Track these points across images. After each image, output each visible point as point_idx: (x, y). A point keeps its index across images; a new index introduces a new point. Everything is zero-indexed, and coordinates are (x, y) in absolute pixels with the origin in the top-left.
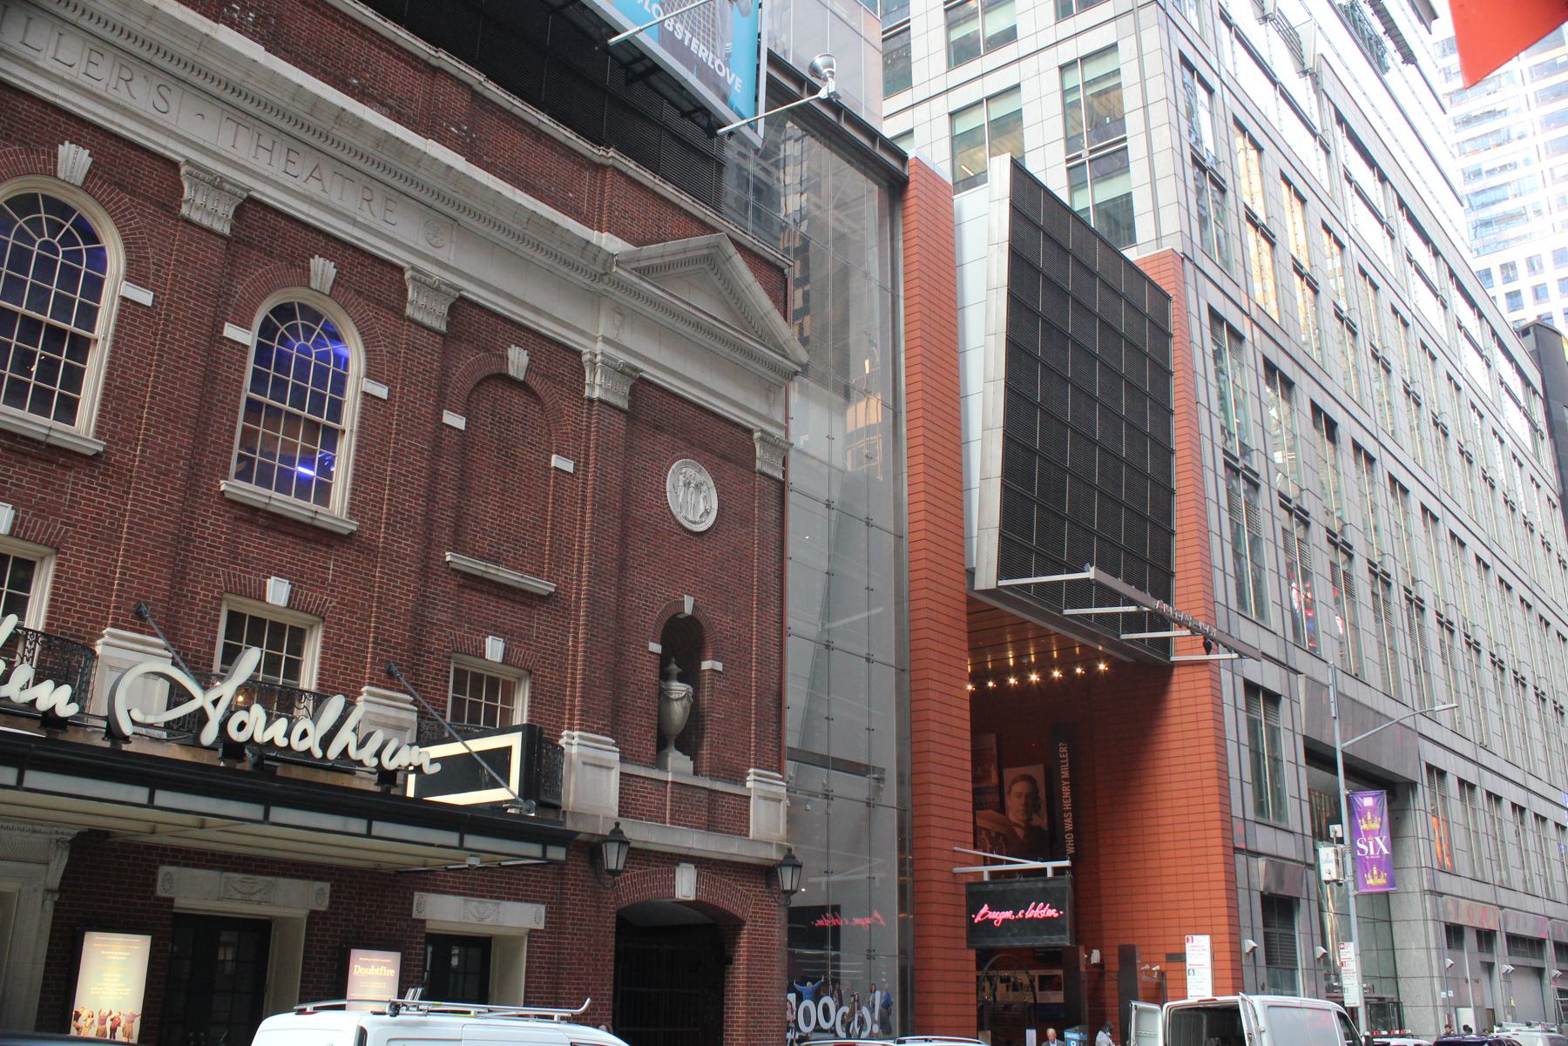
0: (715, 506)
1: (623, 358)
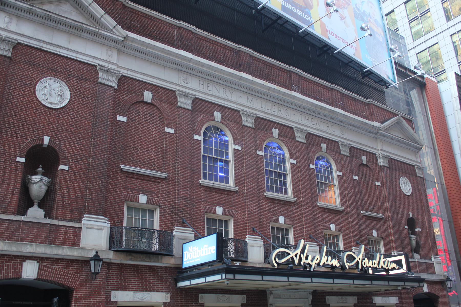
0: (411, 187)
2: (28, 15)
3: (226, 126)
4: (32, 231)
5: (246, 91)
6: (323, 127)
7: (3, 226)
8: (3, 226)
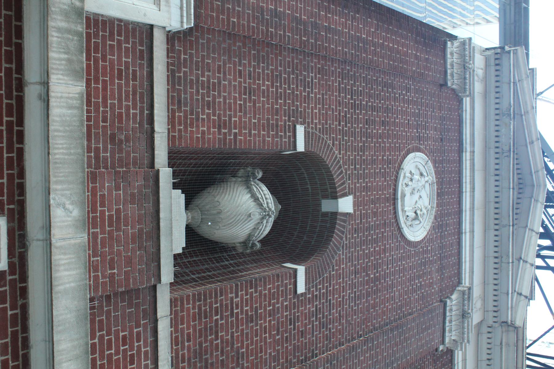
2: (493, 112)
4: (126, 216)
7: (127, 99)
8: (127, 99)
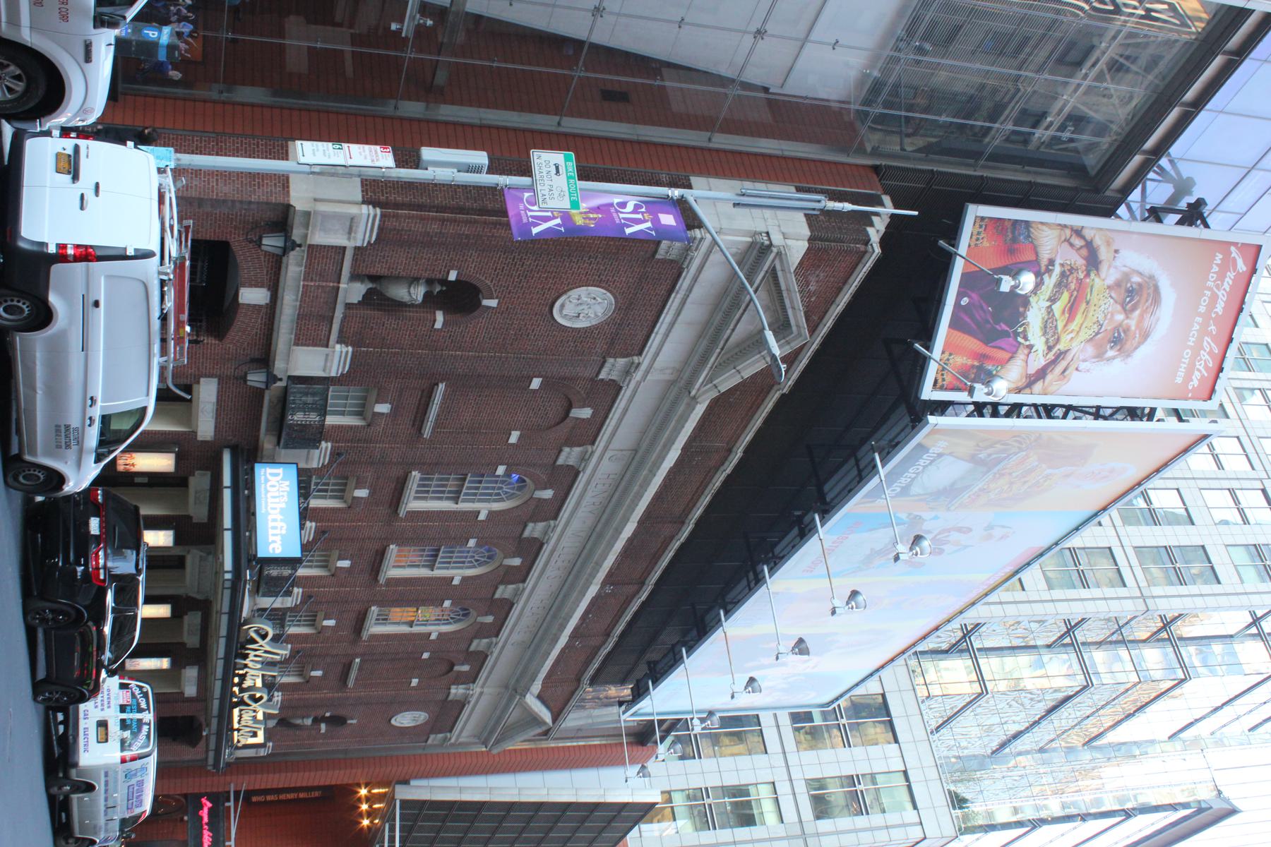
1: (473, 701)
3: (526, 502)
5: (598, 529)
6: (527, 620)
